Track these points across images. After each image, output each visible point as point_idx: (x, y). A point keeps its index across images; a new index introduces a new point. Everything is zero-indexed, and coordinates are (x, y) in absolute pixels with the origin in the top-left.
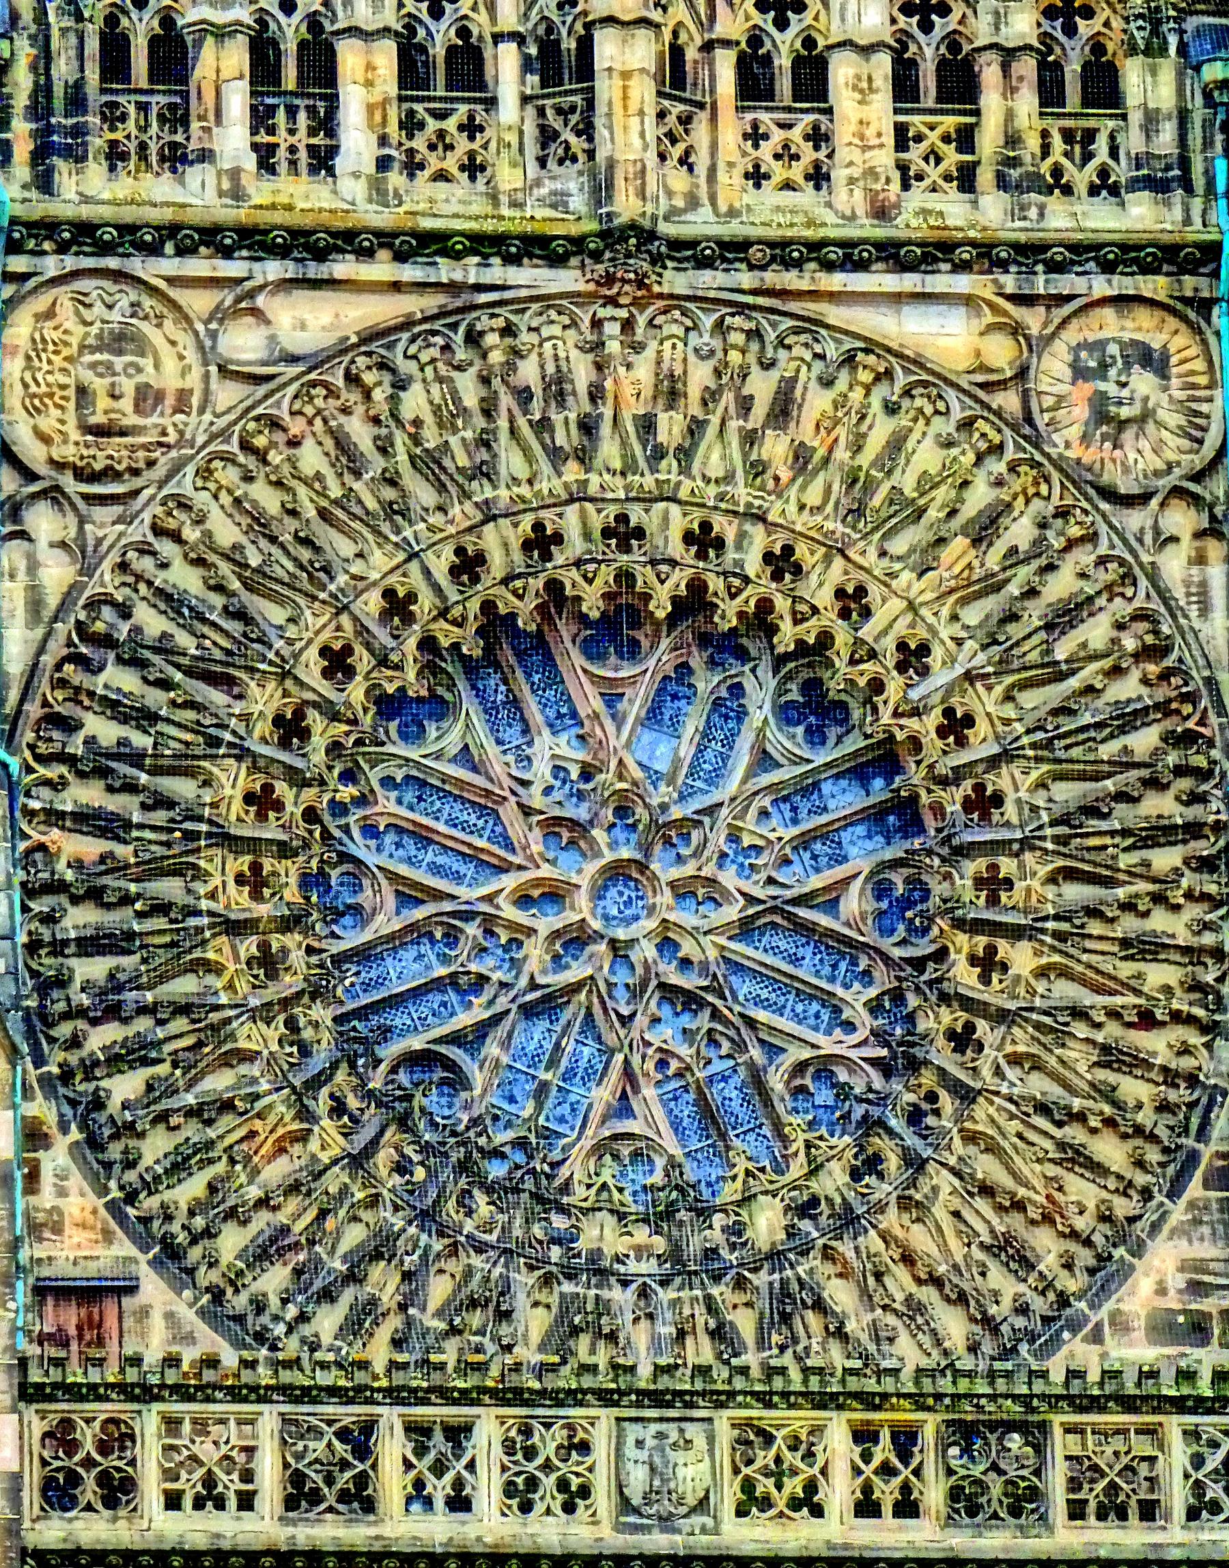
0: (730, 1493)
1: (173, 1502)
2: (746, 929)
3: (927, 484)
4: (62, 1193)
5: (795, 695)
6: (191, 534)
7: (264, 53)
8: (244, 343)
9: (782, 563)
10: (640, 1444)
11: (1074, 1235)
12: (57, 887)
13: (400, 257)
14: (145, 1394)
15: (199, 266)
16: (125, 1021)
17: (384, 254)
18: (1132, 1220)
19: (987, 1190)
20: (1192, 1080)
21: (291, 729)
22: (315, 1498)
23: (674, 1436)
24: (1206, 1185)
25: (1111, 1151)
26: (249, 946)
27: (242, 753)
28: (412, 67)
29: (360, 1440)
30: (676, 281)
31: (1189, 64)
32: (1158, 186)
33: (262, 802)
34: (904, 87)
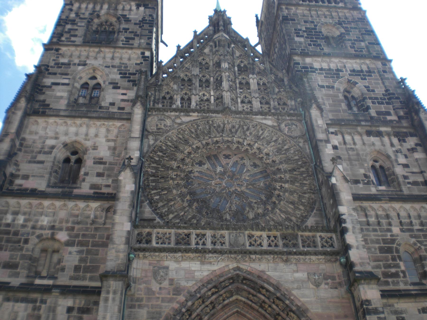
0: (248, 244)
1: (157, 243)
3: (267, 136)
7: (182, 99)
8: (178, 121)
10: (233, 236)
12: (149, 175)
14: (154, 227)
15: (173, 113)
17: (196, 112)
18: (306, 216)
21: (183, 160)
22: (180, 243)
23: (238, 235)
24: (316, 211)
25: (301, 207)
26: (176, 182)
29: (188, 235)
31: (296, 101)
32: (294, 111)
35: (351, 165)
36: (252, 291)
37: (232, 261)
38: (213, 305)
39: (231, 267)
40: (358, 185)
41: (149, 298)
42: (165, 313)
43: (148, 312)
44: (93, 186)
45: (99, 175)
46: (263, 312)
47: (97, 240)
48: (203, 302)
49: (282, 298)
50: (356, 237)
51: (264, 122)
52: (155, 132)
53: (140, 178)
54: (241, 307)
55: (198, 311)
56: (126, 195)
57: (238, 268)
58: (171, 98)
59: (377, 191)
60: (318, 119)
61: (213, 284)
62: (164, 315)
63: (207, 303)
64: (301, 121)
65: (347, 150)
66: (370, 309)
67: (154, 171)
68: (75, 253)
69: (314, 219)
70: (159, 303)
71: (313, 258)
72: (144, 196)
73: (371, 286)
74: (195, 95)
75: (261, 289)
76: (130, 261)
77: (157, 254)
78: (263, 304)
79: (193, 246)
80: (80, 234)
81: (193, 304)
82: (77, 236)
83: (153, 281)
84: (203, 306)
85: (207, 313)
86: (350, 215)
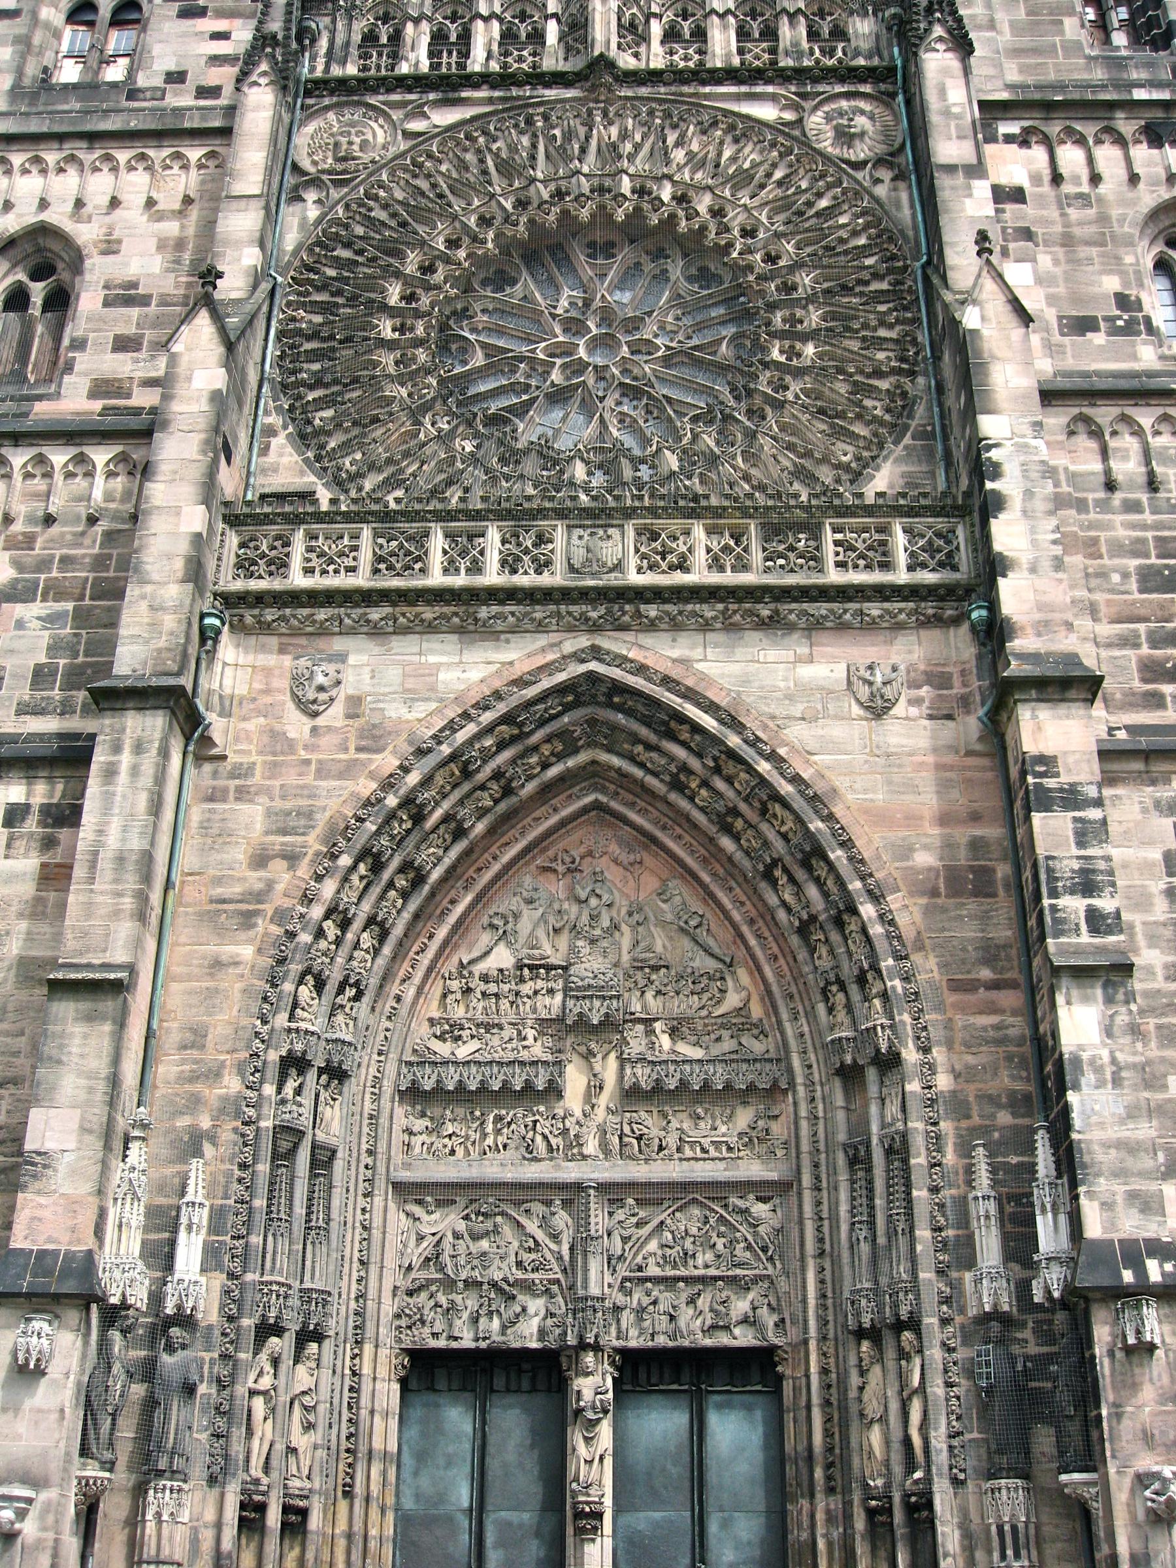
2: (667, 361)
3: (755, 165)
4: (281, 455)
5: (694, 271)
6: (382, 193)
9: (681, 199)
11: (839, 466)
12: (299, 332)
13: (493, 87)
16: (380, 470)
19: (790, 447)
20: (904, 394)
25: (859, 429)
27: (398, 274)
28: (509, 36)
30: (626, 92)
33: (410, 298)
34: (743, 34)
35: (1068, 261)
36: (644, 732)
37: (571, 629)
38: (503, 782)
39: (569, 647)
40: (1089, 335)
41: (275, 764)
42: (328, 814)
43: (269, 813)
44: (102, 388)
45: (123, 344)
46: (684, 804)
47: (111, 574)
48: (467, 774)
49: (748, 753)
50: (1033, 530)
51: (747, 108)
52: (329, 172)
53: (265, 348)
54: (612, 787)
55: (446, 805)
56: (195, 408)
57: (596, 653)
58: (396, 37)
59: (1162, 358)
60: (949, 83)
61: (502, 708)
62: (322, 819)
63: (481, 777)
64: (893, 95)
65: (1064, 202)
66: (1050, 790)
67: (318, 319)
68: (38, 624)
69: (905, 468)
70: (309, 779)
71: (874, 609)
72: (279, 409)
73: (1062, 709)
74: (486, 19)
75: (673, 724)
76: (209, 637)
77: (305, 612)
78: (682, 777)
79: (436, 578)
80: (53, 556)
81: (426, 782)
82: (44, 564)
83: (290, 705)
84: (466, 787)
85: (482, 813)
86: (1023, 448)
